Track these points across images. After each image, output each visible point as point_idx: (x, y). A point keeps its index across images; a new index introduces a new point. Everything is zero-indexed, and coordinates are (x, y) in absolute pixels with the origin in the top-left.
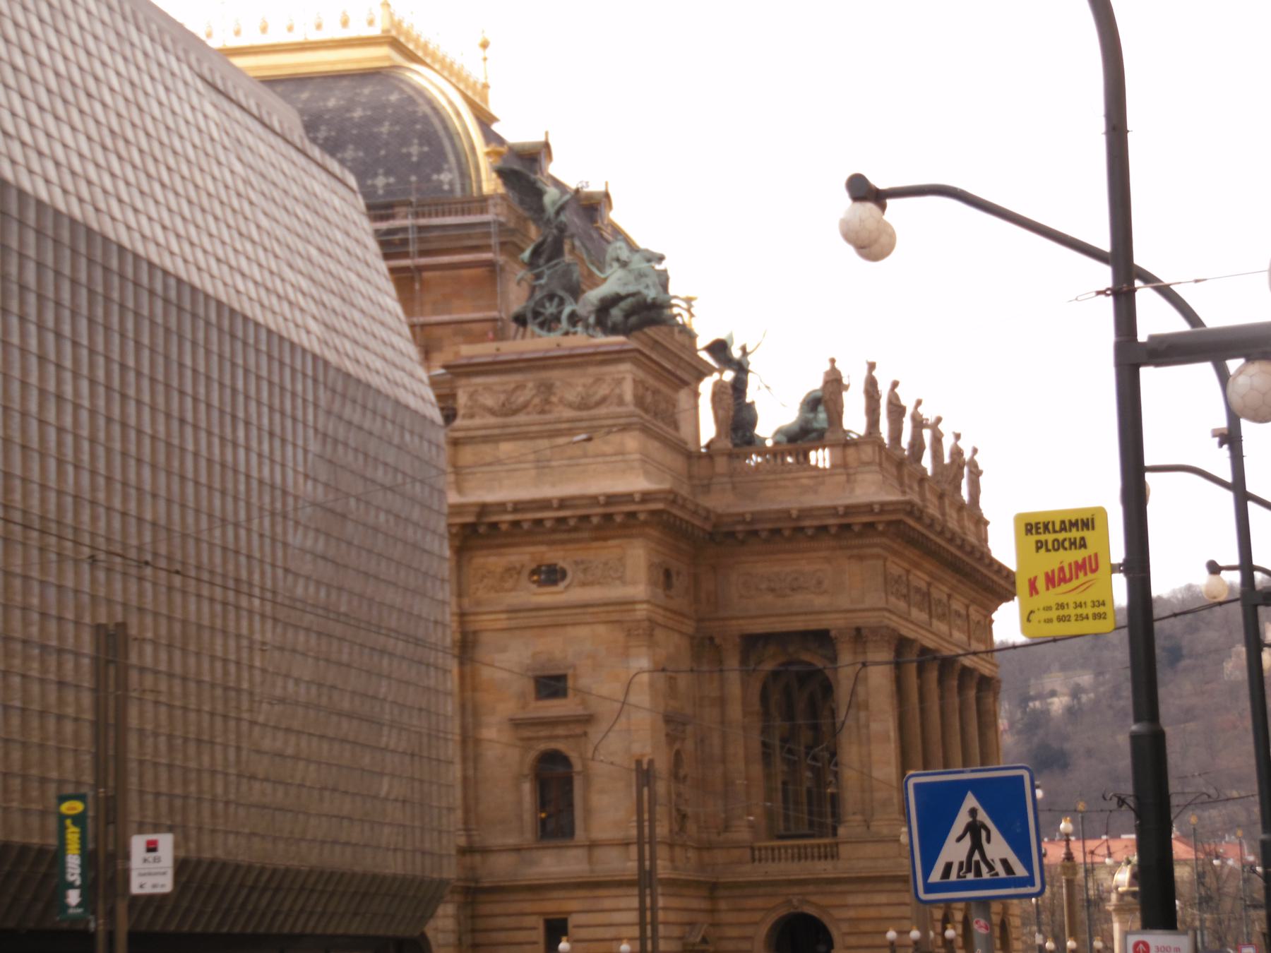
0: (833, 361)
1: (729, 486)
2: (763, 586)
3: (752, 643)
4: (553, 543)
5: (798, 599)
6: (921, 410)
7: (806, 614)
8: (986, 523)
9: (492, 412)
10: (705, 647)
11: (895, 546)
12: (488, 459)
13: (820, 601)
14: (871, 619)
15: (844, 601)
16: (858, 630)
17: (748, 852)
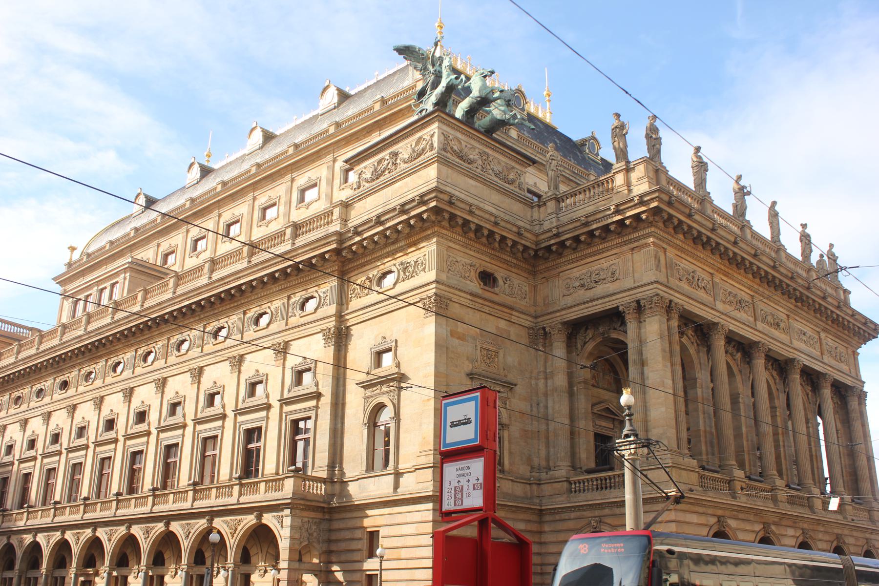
0: (618, 115)
1: (554, 220)
2: (577, 284)
3: (575, 329)
4: (388, 255)
5: (600, 290)
6: (742, 183)
7: (603, 297)
8: (847, 292)
9: (367, 181)
10: (539, 337)
11: (679, 243)
12: (362, 211)
13: (611, 287)
14: (649, 291)
15: (628, 283)
16: (638, 302)
17: (565, 484)
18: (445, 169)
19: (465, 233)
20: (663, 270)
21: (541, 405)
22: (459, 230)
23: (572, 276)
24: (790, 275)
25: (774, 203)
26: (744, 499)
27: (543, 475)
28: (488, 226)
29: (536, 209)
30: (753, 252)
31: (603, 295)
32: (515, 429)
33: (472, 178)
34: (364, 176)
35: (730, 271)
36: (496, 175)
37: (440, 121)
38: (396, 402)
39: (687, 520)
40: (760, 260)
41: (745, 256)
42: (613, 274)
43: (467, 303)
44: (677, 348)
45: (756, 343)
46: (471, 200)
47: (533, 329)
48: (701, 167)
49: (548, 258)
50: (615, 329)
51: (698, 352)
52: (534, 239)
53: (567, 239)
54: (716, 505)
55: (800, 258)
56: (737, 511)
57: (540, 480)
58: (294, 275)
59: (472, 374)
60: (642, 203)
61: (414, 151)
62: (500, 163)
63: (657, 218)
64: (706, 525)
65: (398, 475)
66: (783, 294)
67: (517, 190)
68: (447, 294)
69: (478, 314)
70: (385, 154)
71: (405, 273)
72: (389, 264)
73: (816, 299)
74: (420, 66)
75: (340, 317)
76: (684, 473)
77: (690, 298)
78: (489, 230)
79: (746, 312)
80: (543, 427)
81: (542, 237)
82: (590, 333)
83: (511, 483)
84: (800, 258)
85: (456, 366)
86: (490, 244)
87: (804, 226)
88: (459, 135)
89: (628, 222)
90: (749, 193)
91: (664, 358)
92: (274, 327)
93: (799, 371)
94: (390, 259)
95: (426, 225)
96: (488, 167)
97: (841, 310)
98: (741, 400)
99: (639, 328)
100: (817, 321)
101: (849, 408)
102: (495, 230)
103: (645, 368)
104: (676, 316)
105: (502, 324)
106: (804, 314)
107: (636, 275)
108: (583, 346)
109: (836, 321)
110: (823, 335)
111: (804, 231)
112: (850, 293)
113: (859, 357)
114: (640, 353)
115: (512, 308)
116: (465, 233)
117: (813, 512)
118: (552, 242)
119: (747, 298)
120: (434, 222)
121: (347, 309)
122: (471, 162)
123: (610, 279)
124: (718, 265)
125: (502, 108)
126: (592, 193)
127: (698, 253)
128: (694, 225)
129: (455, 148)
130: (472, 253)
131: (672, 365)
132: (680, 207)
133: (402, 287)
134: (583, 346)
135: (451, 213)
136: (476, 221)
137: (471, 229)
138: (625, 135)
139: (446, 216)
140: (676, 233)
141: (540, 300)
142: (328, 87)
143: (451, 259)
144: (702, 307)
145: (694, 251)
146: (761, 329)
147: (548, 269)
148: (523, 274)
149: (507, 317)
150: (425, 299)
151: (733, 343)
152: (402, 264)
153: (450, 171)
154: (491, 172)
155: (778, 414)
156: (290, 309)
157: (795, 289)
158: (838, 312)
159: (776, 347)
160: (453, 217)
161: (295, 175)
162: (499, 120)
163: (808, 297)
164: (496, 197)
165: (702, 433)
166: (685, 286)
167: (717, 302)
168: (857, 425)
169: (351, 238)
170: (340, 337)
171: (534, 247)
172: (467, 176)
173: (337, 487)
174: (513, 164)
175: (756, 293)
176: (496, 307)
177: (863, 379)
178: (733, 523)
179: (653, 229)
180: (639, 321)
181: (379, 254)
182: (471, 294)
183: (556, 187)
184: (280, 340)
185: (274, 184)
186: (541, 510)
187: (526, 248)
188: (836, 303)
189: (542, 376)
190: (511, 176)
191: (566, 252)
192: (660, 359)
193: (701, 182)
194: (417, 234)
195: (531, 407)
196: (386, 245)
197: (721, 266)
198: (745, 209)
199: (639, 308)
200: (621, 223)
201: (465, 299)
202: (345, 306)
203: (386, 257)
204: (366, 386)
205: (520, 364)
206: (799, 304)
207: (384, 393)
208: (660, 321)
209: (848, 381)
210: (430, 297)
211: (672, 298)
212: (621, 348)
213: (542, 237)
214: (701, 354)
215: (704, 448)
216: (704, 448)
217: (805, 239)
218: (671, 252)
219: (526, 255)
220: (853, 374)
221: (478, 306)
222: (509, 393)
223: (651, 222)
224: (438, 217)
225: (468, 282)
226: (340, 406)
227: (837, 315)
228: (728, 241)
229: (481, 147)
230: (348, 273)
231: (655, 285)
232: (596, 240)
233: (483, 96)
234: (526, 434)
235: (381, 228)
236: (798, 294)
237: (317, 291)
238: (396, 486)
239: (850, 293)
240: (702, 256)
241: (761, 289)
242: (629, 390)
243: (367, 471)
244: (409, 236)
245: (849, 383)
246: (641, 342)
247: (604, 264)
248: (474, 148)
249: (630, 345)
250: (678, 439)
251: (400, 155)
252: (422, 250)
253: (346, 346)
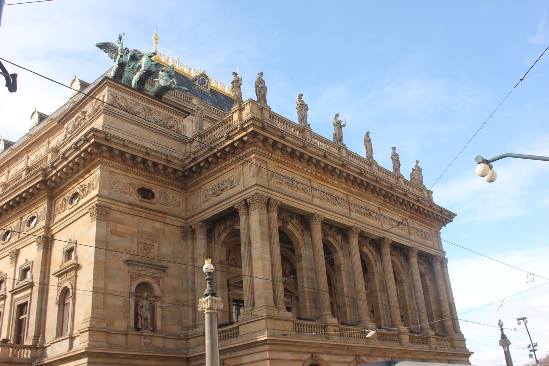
0: (235, 74)
2: (210, 193)
3: (213, 224)
8: (430, 192)
9: (70, 134)
10: (188, 233)
13: (231, 192)
14: (252, 192)
15: (240, 188)
16: (245, 200)
18: (111, 119)
19: (124, 161)
20: (265, 177)
21: (190, 281)
22: (119, 159)
23: (208, 188)
24: (375, 179)
25: (368, 133)
26: (336, 339)
27: (190, 332)
28: (140, 155)
29: (188, 144)
30: (341, 163)
31: (225, 198)
32: (168, 299)
33: (133, 124)
34: (69, 130)
35: (325, 177)
36: (157, 123)
37: (109, 86)
38: (73, 285)
39: (281, 358)
40: (348, 169)
41: (335, 166)
42: (232, 183)
43: (127, 210)
44: (276, 233)
45: (350, 228)
46: (124, 137)
47: (184, 227)
48: (303, 108)
49: (192, 177)
50: (237, 222)
51: (303, 236)
52: (181, 163)
53: (201, 162)
54: (310, 345)
55: (392, 171)
56: (330, 348)
57: (188, 336)
58: (21, 203)
59: (127, 261)
60: (243, 129)
61: (94, 108)
62: (160, 115)
63: (255, 140)
64: (300, 360)
65: (72, 338)
66: (373, 193)
68: (108, 204)
69: (136, 219)
70: (79, 114)
71: (83, 193)
72: (76, 188)
73: (399, 196)
74: (114, 55)
75: (48, 228)
76: (279, 323)
77: (288, 196)
78: (143, 159)
79: (341, 206)
80: (191, 297)
81: (186, 162)
82: (222, 227)
83: (162, 339)
84: (392, 171)
85: (115, 256)
86: (146, 168)
87: (394, 149)
88: (126, 96)
89: (236, 144)
90: (344, 126)
91: (262, 239)
92: (12, 241)
93: (389, 246)
94: (76, 184)
95: (93, 156)
96: (150, 117)
97: (421, 203)
98: (342, 268)
99: (248, 219)
100: (404, 211)
101: (435, 270)
102: (147, 158)
103: (253, 248)
104: (276, 209)
105: (158, 225)
106: (393, 207)
107: (245, 182)
108: (219, 237)
109: (418, 210)
110: (410, 221)
111: (394, 152)
112: (432, 192)
113: (441, 235)
114: (249, 237)
115: (165, 213)
116: (124, 161)
117: (402, 345)
118: (192, 164)
119: (342, 196)
120: (97, 154)
121: (53, 222)
122: (135, 114)
123: (230, 187)
124: (315, 173)
125: (165, 78)
126: (221, 129)
127: (295, 165)
128: (287, 144)
129: (122, 104)
130: (132, 175)
131: (271, 244)
132: (273, 131)
133: (82, 202)
134: (219, 237)
135: (109, 147)
136: (130, 151)
137: (126, 157)
138: (239, 87)
139: (104, 148)
140: (274, 150)
141: (189, 206)
142: (74, 80)
143: (113, 180)
144: (299, 202)
145: (292, 163)
146: (355, 218)
147: (194, 185)
148: (177, 189)
149: (161, 219)
150: (91, 209)
151: (334, 229)
152: (81, 186)
153: (115, 119)
155: (376, 277)
156: (22, 227)
157: (381, 189)
158: (419, 205)
159: (367, 230)
160: (110, 150)
161: (50, 139)
162: (164, 87)
163: (392, 195)
164: (155, 137)
165: (306, 293)
166: (285, 188)
167: (314, 199)
168: (441, 282)
169: (51, 172)
170: (47, 242)
171: (182, 169)
172: (130, 122)
173: (39, 351)
174: (172, 115)
175: (350, 192)
176: (152, 213)
177: (445, 250)
178: (326, 358)
179: (254, 148)
180: (248, 214)
181: (70, 181)
182: (129, 204)
183: (201, 128)
184: (13, 249)
185: (39, 147)
186: (188, 358)
187: (175, 171)
188: (416, 198)
189: (190, 260)
190: (171, 123)
191: (204, 171)
192: (259, 240)
193: (303, 117)
194: (89, 164)
195: (183, 283)
196: (73, 175)
197: (317, 174)
198: (342, 137)
199: (247, 205)
200: (232, 145)
201: (124, 208)
202: (52, 221)
203: (74, 183)
204: (59, 275)
205: (173, 253)
206: (387, 200)
207: (67, 280)
208: (259, 212)
209: (432, 252)
210: (93, 207)
211: (270, 196)
212: (236, 234)
213: (186, 162)
214: (305, 237)
215: (308, 304)
216: (308, 304)
217: (395, 158)
218: (272, 165)
219: (176, 176)
220: (436, 247)
221: (136, 213)
222: (163, 275)
223: (252, 143)
224: (101, 149)
225: (128, 196)
226: (45, 292)
227: (418, 206)
228: (319, 155)
229: (144, 103)
230: (55, 197)
231: (256, 187)
232: (220, 160)
233: (147, 69)
234: (178, 304)
235: (66, 162)
236: (384, 192)
237: (36, 212)
238: (71, 347)
239: (432, 192)
240: (300, 167)
241: (354, 190)
242: (210, 261)
243: (57, 337)
244: (84, 167)
245: (433, 253)
246: (249, 229)
247: (227, 177)
248: (138, 104)
249: (242, 232)
250: (275, 298)
251: (88, 113)
252: (93, 175)
253: (51, 248)
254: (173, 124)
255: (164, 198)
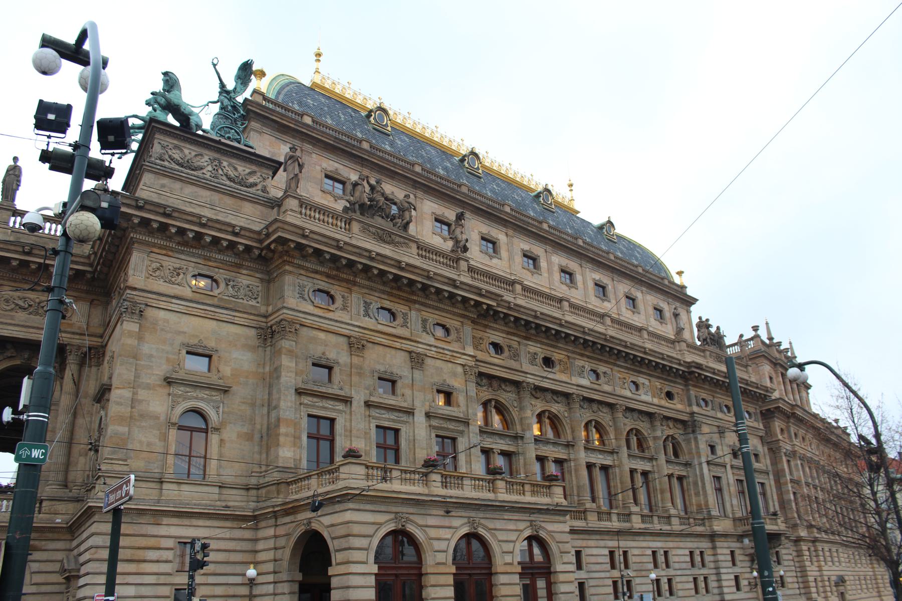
29: (276, 209)
67: (260, 192)
96: (220, 172)
129: (176, 156)
154: (224, 178)
254: (258, 181)
255: (233, 287)
